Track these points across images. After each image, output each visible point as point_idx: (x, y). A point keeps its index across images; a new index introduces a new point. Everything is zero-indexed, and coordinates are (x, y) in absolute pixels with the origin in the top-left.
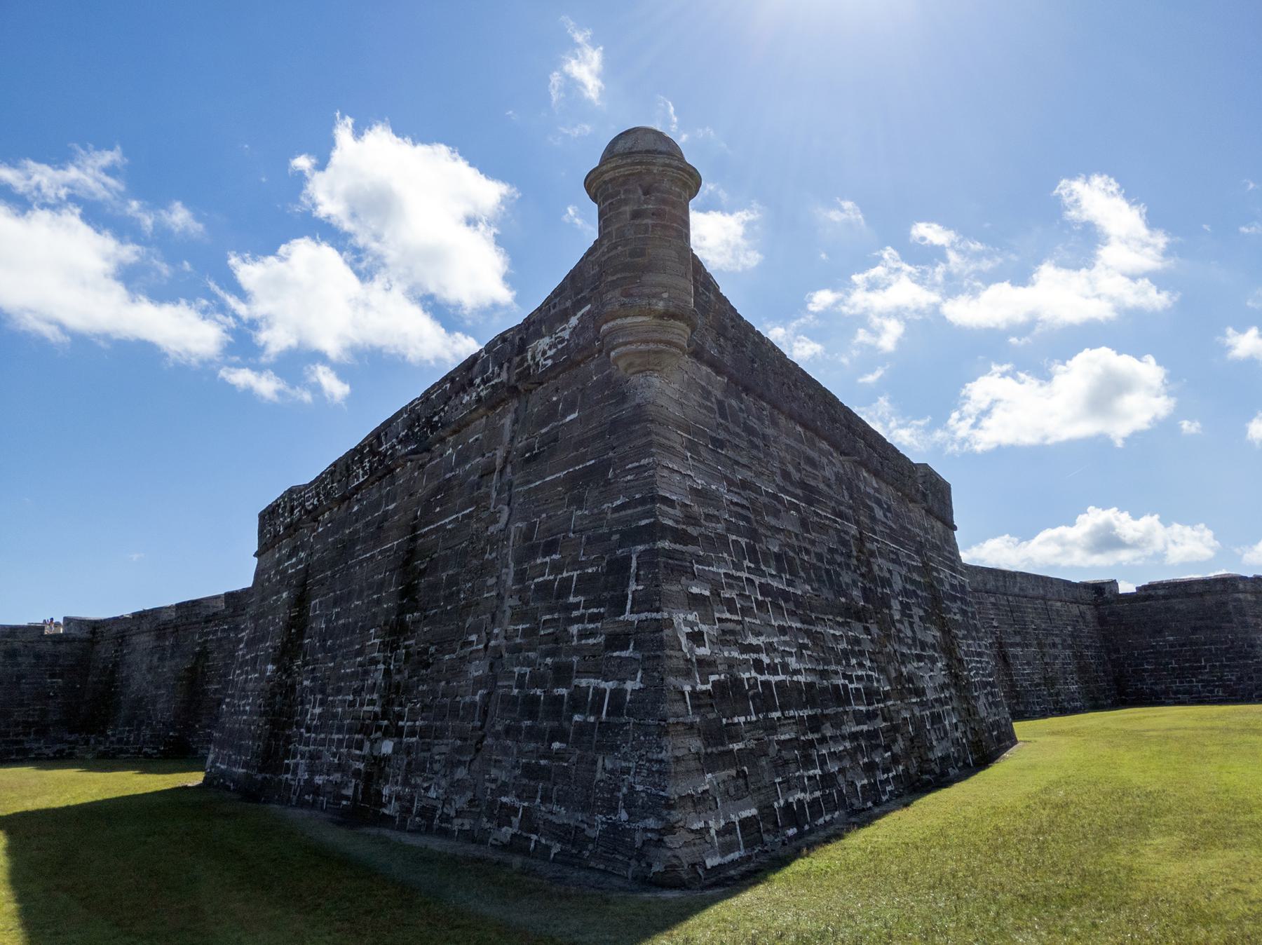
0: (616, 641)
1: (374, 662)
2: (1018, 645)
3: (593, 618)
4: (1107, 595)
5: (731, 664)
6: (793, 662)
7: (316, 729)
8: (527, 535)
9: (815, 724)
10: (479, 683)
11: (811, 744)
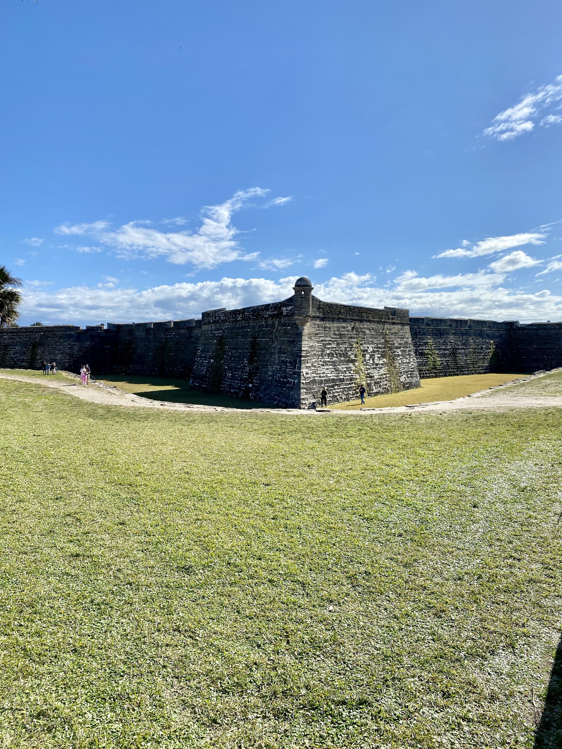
0: (294, 373)
1: (246, 366)
2: (462, 349)
3: (291, 369)
4: (514, 327)
5: (314, 377)
6: (329, 375)
7: (230, 379)
8: (280, 349)
9: (333, 386)
10: (271, 376)
11: (331, 390)
